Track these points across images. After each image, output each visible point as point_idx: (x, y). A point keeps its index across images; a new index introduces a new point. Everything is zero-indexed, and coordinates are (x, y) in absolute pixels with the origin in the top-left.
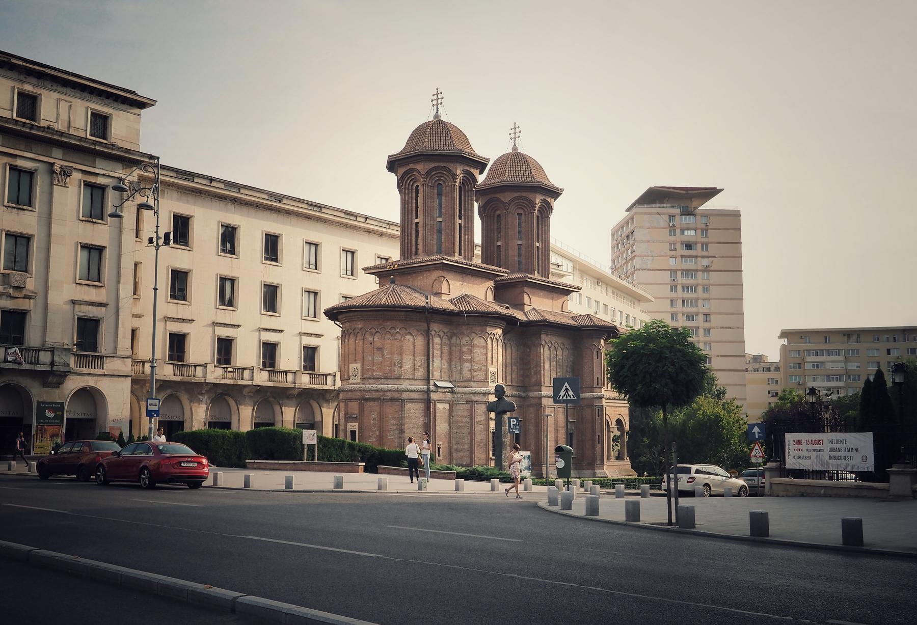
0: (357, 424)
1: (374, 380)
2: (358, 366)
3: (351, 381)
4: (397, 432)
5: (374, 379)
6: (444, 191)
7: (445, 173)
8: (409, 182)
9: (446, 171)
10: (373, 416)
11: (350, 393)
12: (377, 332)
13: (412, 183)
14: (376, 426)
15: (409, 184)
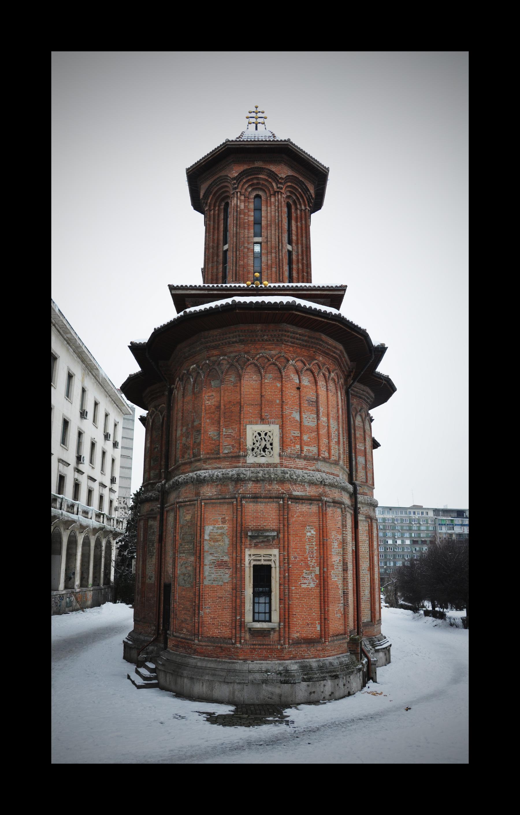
0: (275, 552)
1: (305, 462)
2: (274, 430)
3: (251, 459)
4: (340, 569)
5: (306, 458)
6: (294, 215)
7: (300, 190)
8: (247, 186)
9: (301, 189)
10: (309, 534)
11: (250, 485)
12: (307, 370)
13: (250, 190)
14: (315, 555)
15: (246, 190)
